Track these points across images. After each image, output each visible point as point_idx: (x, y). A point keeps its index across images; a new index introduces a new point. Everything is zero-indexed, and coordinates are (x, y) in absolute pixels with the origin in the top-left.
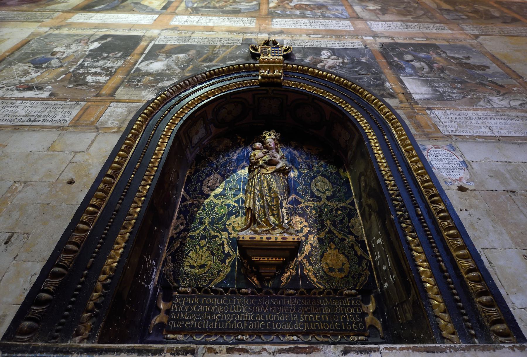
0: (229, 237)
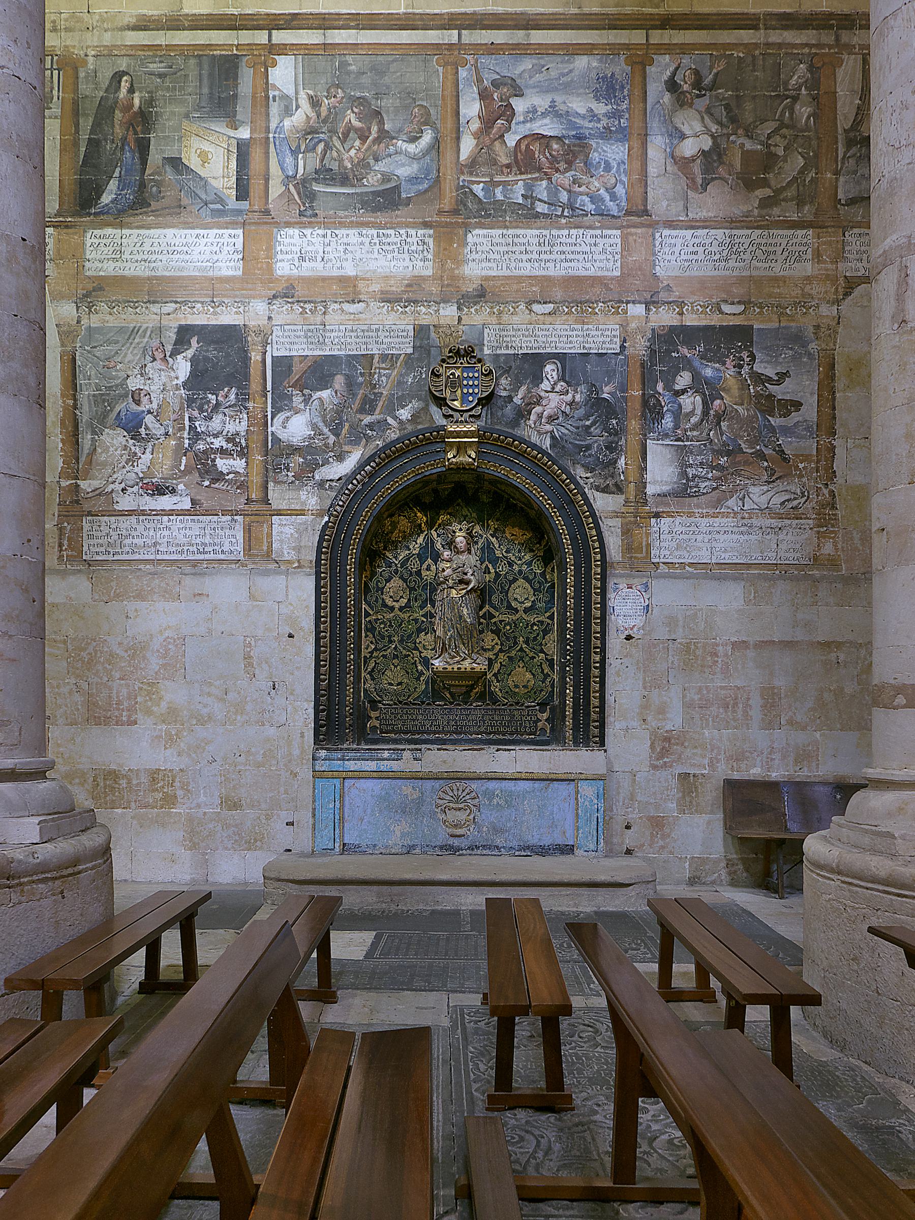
0: (420, 656)
